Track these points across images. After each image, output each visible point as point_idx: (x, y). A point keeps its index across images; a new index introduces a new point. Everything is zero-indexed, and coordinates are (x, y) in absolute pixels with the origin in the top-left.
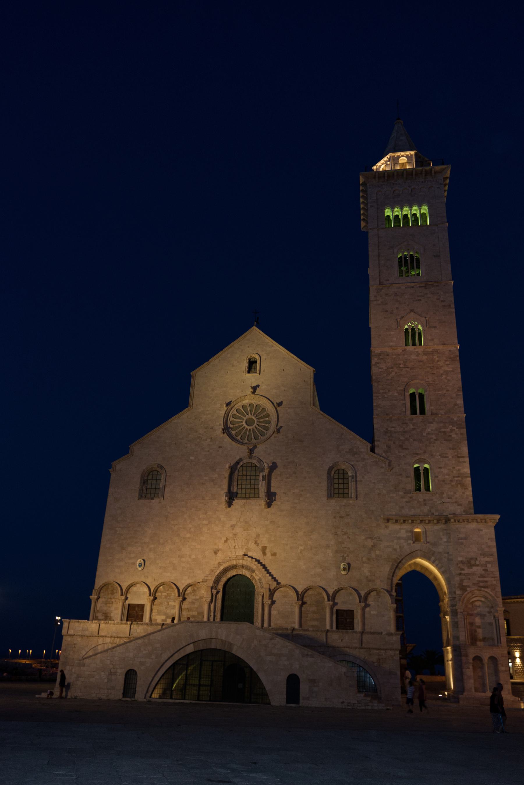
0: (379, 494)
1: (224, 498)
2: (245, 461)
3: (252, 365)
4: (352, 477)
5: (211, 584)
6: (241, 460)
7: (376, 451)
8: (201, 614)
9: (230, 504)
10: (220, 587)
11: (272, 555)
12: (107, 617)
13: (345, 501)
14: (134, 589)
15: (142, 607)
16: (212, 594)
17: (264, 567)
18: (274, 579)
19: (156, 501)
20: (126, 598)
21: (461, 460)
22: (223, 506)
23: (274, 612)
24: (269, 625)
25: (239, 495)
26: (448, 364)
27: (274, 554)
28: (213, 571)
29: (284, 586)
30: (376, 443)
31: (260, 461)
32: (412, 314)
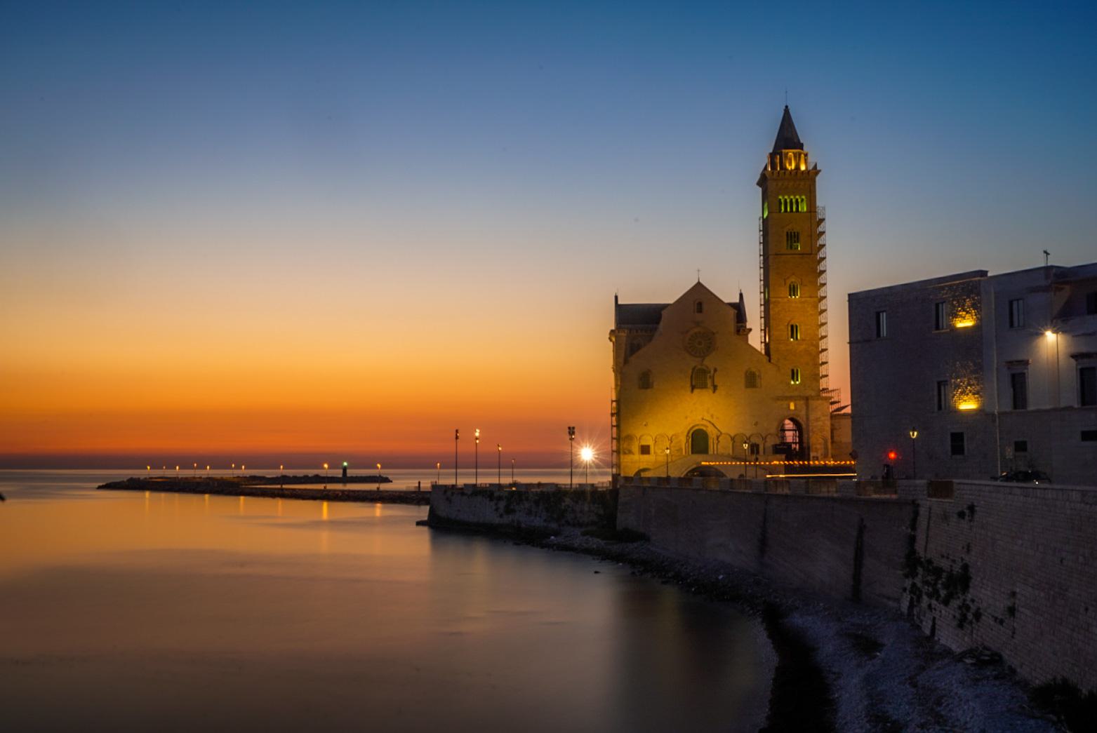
1: (690, 389)
5: (686, 434)
7: (772, 361)
8: (681, 449)
10: (690, 435)
12: (630, 452)
13: (754, 389)
14: (643, 438)
15: (648, 446)
17: (713, 424)
18: (719, 430)
19: (649, 390)
22: (689, 392)
23: (719, 447)
27: (717, 418)
30: (772, 357)
31: (707, 367)
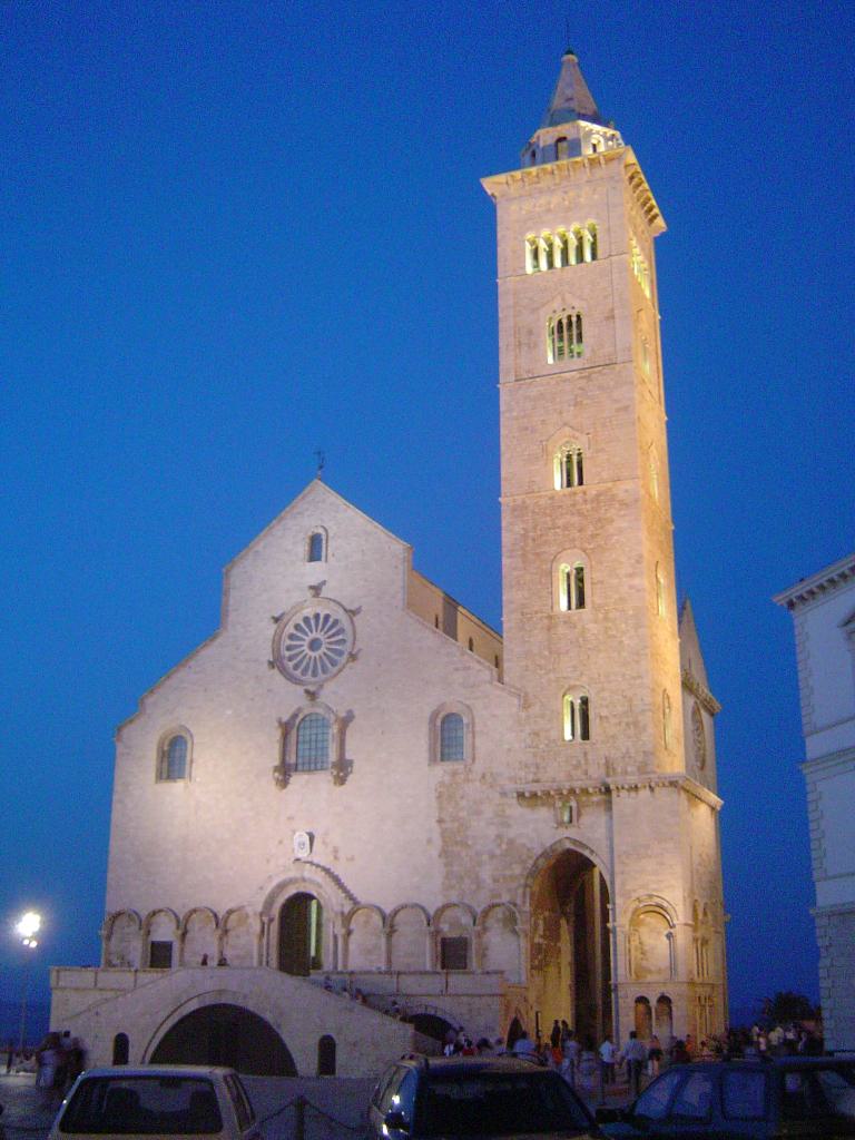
0: (509, 750)
2: (306, 712)
3: (315, 549)
4: (468, 725)
6: (300, 710)
7: (506, 679)
9: (283, 783)
11: (348, 859)
16: (263, 924)
20: (149, 933)
21: (638, 682)
23: (352, 947)
24: (345, 965)
25: (300, 767)
26: (624, 515)
28: (261, 888)
29: (364, 908)
32: (567, 429)
